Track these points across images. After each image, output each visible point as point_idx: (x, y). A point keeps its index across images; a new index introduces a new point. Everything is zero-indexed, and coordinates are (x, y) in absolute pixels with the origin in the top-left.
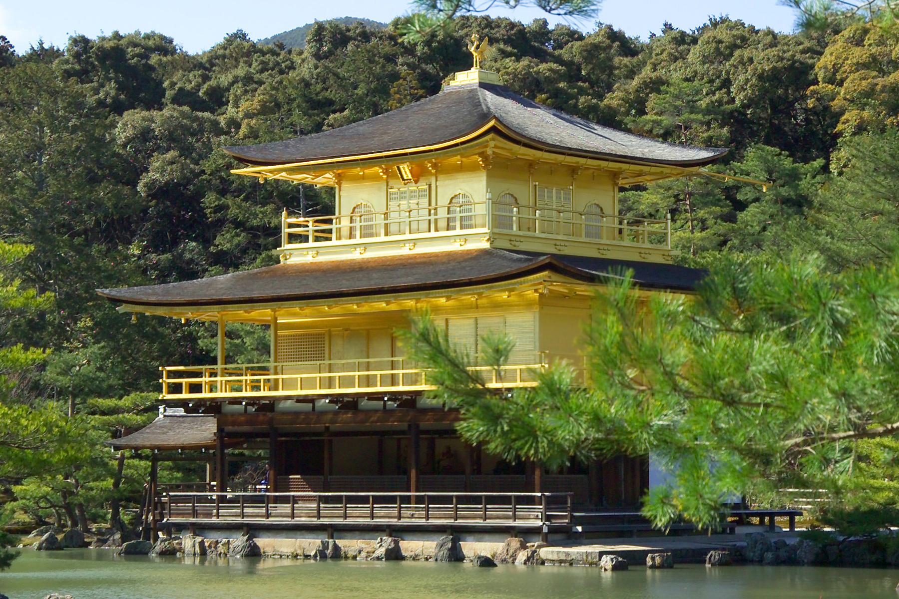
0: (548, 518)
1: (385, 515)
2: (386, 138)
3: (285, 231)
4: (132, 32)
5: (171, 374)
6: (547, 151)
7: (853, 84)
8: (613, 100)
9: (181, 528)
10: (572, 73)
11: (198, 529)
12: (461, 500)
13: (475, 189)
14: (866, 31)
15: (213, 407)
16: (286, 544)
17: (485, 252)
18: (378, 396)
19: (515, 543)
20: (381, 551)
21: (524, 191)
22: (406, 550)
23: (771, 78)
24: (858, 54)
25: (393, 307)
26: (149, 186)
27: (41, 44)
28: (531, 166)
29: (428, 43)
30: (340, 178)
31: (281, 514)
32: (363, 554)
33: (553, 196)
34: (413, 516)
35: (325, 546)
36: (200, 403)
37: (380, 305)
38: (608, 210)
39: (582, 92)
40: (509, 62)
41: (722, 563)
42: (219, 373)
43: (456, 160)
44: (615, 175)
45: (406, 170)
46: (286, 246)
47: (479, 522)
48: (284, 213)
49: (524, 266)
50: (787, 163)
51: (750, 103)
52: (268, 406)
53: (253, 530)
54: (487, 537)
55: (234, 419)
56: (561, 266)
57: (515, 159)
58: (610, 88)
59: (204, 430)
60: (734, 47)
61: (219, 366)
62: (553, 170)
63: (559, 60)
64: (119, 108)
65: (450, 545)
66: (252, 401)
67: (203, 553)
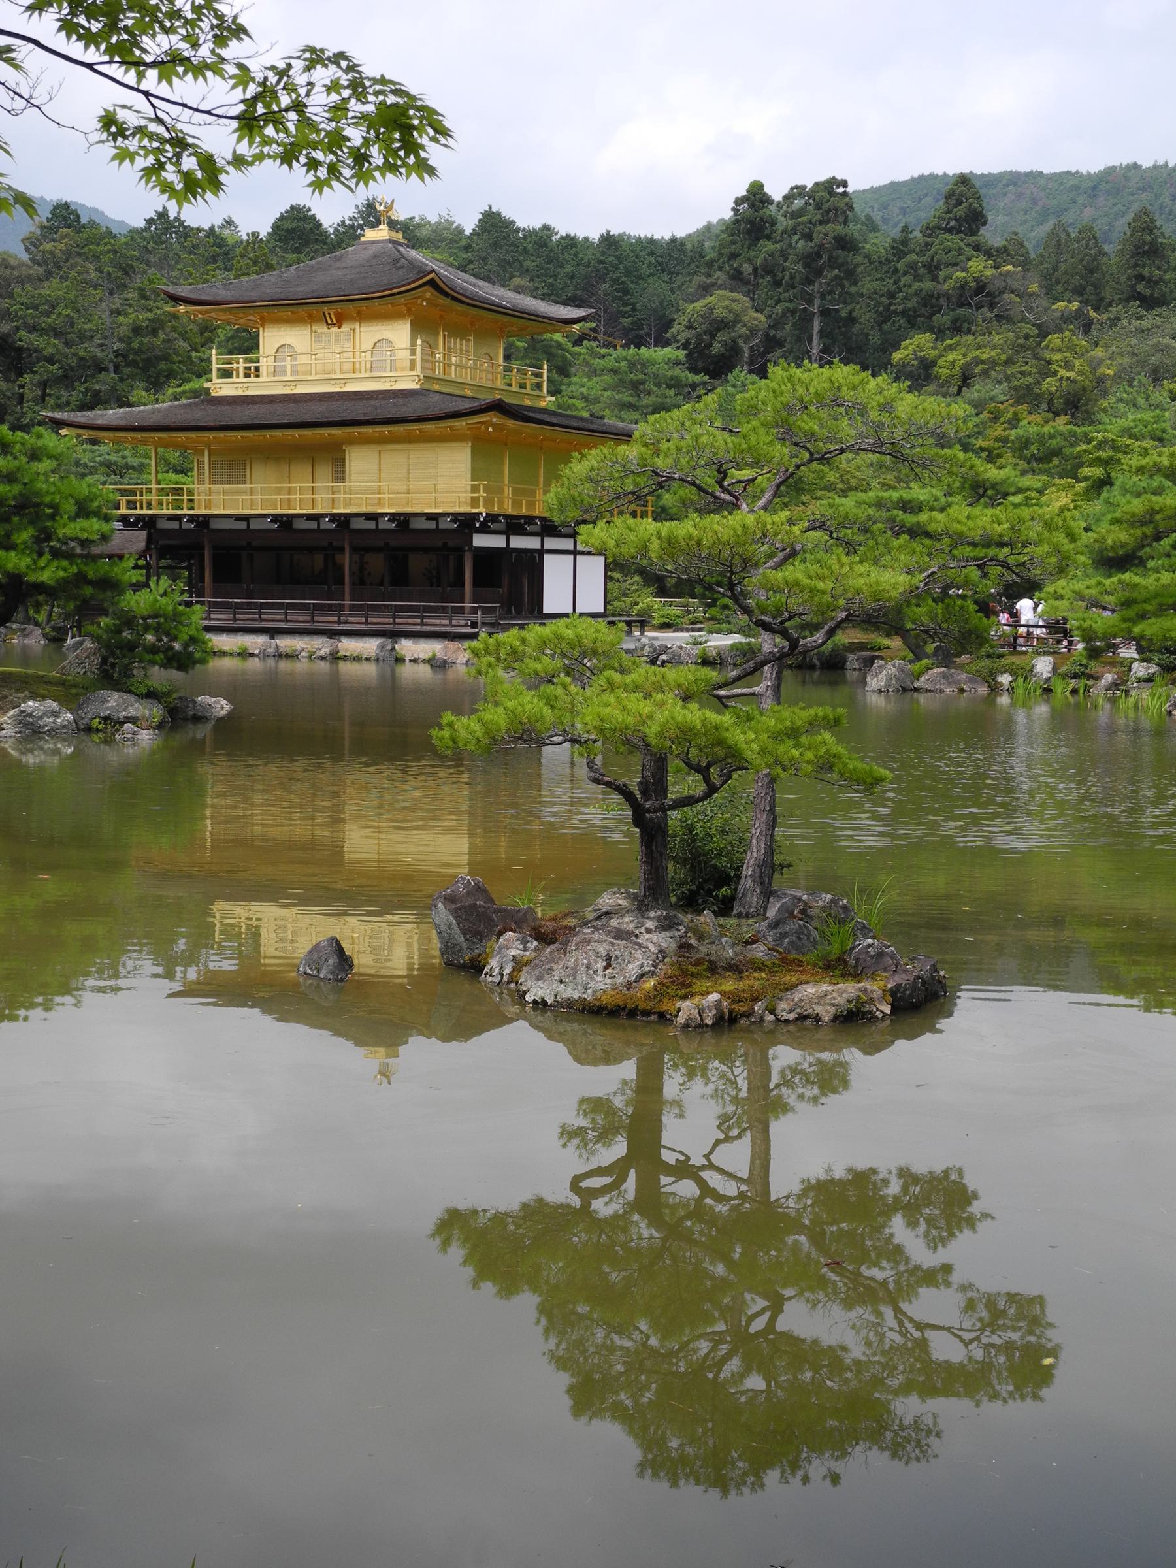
1: (329, 620)
3: (215, 366)
6: (469, 304)
15: (149, 523)
18: (316, 517)
19: (452, 645)
20: (325, 651)
22: (346, 650)
30: (264, 322)
32: (303, 654)
36: (140, 518)
42: (154, 491)
46: (215, 380)
47: (418, 629)
52: (203, 522)
54: (422, 640)
65: (389, 647)
66: (192, 519)
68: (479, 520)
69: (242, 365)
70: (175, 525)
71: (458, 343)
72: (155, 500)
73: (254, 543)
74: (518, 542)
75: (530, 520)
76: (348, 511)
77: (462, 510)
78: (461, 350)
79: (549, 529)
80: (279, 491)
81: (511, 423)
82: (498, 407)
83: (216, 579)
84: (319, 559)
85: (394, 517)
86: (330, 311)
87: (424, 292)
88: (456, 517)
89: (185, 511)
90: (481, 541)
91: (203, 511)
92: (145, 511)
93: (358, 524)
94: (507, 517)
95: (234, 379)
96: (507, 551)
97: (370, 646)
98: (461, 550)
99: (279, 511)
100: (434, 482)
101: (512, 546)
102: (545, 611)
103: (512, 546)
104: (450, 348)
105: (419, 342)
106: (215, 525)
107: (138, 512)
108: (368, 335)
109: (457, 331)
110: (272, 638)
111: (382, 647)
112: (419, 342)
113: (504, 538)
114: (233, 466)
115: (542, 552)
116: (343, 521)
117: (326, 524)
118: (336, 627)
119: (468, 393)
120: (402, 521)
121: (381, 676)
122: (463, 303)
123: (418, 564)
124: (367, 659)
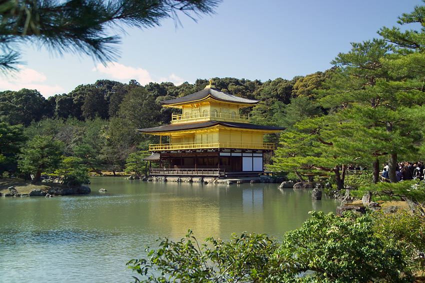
0: (220, 174)
1: (190, 173)
3: (173, 117)
4: (166, 82)
5: (152, 146)
7: (300, 90)
8: (254, 93)
9: (153, 175)
10: (247, 88)
11: (156, 176)
12: (204, 170)
13: (208, 109)
14: (303, 79)
15: (159, 152)
16: (172, 179)
17: (209, 121)
19: (213, 179)
20: (189, 180)
21: (218, 109)
23: (286, 89)
24: (302, 84)
25: (192, 132)
26: (163, 111)
28: (220, 104)
29: (218, 83)
31: (171, 173)
33: (225, 110)
34: (195, 174)
35: (179, 179)
36: (156, 151)
37: (188, 132)
38: (237, 113)
39: (248, 92)
40: (234, 87)
41: (253, 183)
43: (204, 103)
44: (238, 106)
45: (195, 105)
47: (207, 175)
49: (214, 124)
50: (283, 104)
51: (281, 93)
53: (166, 176)
55: (163, 154)
56: (221, 123)
57: (217, 103)
58: (254, 91)
59: (158, 157)
60: (278, 83)
62: (224, 105)
63: (244, 86)
64: (158, 96)
66: (166, 151)
67: (157, 180)
74: (233, 154)
85: (202, 149)
88: (214, 149)
90: (221, 154)
91: (167, 149)
93: (198, 151)
100: (210, 141)
102: (243, 170)
106: (172, 152)
108: (203, 109)
113: (230, 154)
115: (242, 157)
120: (206, 151)
121: (200, 186)
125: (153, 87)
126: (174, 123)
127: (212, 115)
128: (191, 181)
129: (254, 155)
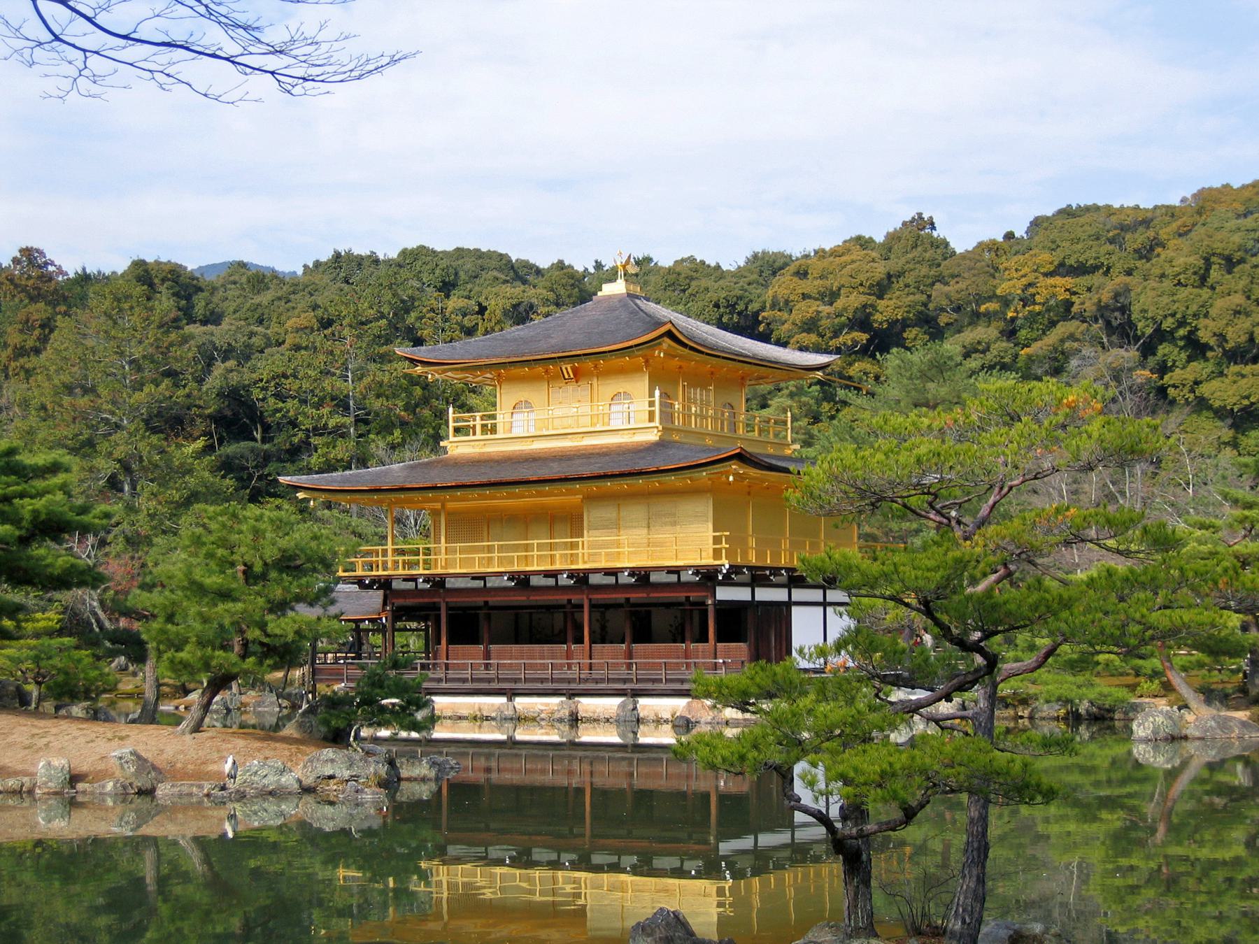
2: (553, 341)
3: (451, 424)
15: (384, 584)
20: (565, 713)
27: (84, 269)
42: (390, 552)
46: (452, 439)
48: (451, 410)
52: (438, 583)
61: (390, 547)
65: (631, 707)
66: (427, 579)
68: (721, 572)
69: (478, 422)
70: (411, 585)
71: (697, 393)
72: (390, 564)
73: (491, 604)
74: (764, 594)
75: (776, 571)
76: (587, 566)
77: (704, 562)
78: (702, 400)
79: (796, 581)
80: (516, 548)
81: (753, 472)
82: (741, 457)
83: (451, 641)
84: (559, 618)
85: (633, 572)
86: (567, 368)
87: (660, 344)
88: (697, 570)
89: (421, 571)
90: (723, 594)
91: (439, 571)
92: (381, 573)
93: (595, 579)
94: (750, 568)
95: (471, 437)
96: (753, 604)
97: (610, 705)
98: (704, 604)
99: (516, 568)
101: (757, 598)
103: (757, 598)
104: (689, 399)
105: (657, 393)
106: (450, 583)
107: (374, 573)
109: (697, 380)
110: (510, 700)
111: (622, 706)
112: (657, 393)
113: (749, 590)
114: (469, 526)
115: (789, 604)
116: (581, 578)
117: (564, 580)
118: (573, 686)
119: (709, 442)
120: (642, 576)
122: (702, 353)
123: (660, 620)
124: (608, 720)
125: (146, 276)
126: (457, 447)
127: (667, 416)
128: (575, 720)
129: (833, 595)
